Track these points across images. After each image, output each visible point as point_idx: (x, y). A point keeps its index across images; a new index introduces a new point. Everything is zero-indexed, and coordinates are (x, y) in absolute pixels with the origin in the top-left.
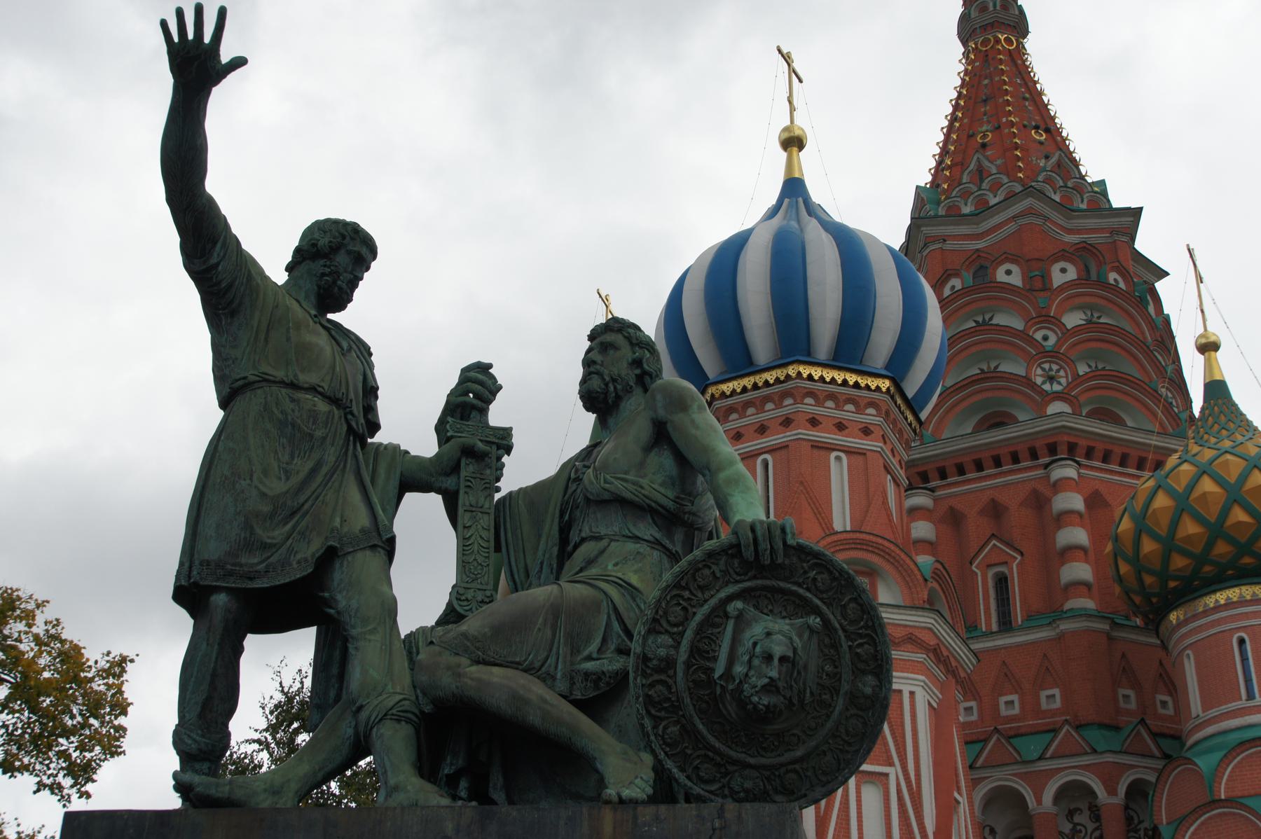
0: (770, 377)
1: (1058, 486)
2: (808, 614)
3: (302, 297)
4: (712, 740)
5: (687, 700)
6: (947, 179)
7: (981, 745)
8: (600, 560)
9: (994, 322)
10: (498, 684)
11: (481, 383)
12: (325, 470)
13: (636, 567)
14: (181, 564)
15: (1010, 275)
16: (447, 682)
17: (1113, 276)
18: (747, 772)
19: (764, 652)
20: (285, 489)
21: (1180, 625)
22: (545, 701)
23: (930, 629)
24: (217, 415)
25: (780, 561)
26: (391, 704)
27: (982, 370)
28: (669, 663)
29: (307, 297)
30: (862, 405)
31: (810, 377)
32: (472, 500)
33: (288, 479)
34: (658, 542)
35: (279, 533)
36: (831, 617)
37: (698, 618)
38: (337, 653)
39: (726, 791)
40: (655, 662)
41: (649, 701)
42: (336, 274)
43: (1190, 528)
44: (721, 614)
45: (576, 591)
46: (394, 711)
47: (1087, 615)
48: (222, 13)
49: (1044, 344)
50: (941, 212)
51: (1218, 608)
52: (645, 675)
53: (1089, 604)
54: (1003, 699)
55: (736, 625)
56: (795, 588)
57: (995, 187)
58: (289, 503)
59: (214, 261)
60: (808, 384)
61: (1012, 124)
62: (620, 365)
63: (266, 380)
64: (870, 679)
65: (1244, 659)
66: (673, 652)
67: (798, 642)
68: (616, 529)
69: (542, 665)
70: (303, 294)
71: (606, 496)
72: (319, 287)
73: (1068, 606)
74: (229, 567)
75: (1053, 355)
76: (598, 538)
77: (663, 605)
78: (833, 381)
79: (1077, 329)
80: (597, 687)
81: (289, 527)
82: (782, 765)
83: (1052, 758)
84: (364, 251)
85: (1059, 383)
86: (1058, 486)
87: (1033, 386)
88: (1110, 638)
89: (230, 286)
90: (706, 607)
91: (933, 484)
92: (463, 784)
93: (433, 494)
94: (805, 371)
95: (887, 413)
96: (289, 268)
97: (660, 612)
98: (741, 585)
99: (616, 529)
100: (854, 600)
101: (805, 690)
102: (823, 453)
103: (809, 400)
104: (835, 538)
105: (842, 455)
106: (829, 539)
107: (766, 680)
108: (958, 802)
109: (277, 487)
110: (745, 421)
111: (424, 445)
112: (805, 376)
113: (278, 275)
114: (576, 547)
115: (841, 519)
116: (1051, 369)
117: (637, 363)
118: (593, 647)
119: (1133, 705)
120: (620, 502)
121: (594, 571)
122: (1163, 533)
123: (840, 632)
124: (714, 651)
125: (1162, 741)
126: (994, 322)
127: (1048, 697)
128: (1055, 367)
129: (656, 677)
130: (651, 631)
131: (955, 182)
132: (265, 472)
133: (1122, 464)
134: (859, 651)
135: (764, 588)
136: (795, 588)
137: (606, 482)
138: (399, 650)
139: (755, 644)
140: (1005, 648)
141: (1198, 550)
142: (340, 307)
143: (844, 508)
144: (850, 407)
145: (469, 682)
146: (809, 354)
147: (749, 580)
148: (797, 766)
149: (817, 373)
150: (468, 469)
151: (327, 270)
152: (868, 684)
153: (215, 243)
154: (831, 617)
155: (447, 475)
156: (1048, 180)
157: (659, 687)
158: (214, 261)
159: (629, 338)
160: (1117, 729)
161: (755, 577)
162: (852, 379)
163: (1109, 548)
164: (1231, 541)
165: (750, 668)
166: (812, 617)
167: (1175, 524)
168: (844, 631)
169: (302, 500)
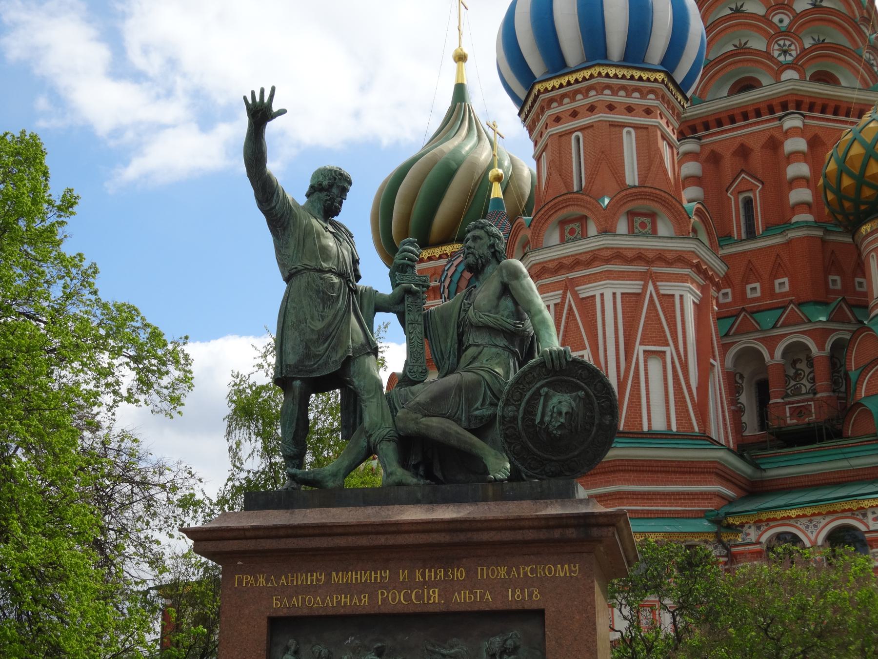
0: (579, 76)
1: (788, 134)
2: (578, 390)
3: (316, 213)
4: (535, 450)
5: (524, 434)
7: (734, 319)
8: (479, 357)
9: (743, 9)
10: (435, 425)
16: (412, 427)
21: (869, 235)
22: (458, 433)
23: (693, 252)
27: (735, 46)
28: (515, 418)
29: (319, 212)
30: (645, 92)
31: (607, 75)
35: (322, 348)
37: (527, 397)
41: (506, 436)
42: (332, 200)
45: (469, 376)
47: (806, 225)
48: (273, 89)
49: (779, 25)
53: (809, 218)
54: (749, 287)
59: (273, 205)
60: (607, 80)
63: (307, 269)
64: (608, 417)
67: (574, 404)
71: (480, 324)
73: (794, 220)
75: (786, 33)
76: (478, 346)
78: (624, 77)
79: (805, 12)
81: (326, 345)
83: (781, 326)
85: (791, 55)
86: (788, 134)
87: (771, 58)
88: (823, 241)
89: (282, 215)
91: (700, 134)
93: (391, 313)
95: (663, 97)
96: (308, 196)
100: (600, 381)
102: (617, 129)
103: (607, 92)
104: (627, 192)
105: (631, 130)
108: (713, 366)
109: (319, 325)
110: (562, 108)
112: (604, 74)
113: (302, 200)
114: (467, 348)
115: (631, 177)
116: (784, 45)
117: (492, 246)
118: (478, 404)
119: (839, 286)
121: (476, 364)
122: (856, 172)
126: (743, 9)
127: (780, 284)
128: (788, 43)
132: (312, 318)
133: (835, 113)
138: (385, 403)
140: (751, 251)
142: (337, 215)
143: (633, 168)
144: (636, 95)
146: (606, 57)
149: (612, 72)
150: (409, 300)
152: (607, 420)
155: (398, 304)
158: (273, 205)
162: (637, 74)
163: (821, 182)
167: (865, 166)
168: (595, 396)
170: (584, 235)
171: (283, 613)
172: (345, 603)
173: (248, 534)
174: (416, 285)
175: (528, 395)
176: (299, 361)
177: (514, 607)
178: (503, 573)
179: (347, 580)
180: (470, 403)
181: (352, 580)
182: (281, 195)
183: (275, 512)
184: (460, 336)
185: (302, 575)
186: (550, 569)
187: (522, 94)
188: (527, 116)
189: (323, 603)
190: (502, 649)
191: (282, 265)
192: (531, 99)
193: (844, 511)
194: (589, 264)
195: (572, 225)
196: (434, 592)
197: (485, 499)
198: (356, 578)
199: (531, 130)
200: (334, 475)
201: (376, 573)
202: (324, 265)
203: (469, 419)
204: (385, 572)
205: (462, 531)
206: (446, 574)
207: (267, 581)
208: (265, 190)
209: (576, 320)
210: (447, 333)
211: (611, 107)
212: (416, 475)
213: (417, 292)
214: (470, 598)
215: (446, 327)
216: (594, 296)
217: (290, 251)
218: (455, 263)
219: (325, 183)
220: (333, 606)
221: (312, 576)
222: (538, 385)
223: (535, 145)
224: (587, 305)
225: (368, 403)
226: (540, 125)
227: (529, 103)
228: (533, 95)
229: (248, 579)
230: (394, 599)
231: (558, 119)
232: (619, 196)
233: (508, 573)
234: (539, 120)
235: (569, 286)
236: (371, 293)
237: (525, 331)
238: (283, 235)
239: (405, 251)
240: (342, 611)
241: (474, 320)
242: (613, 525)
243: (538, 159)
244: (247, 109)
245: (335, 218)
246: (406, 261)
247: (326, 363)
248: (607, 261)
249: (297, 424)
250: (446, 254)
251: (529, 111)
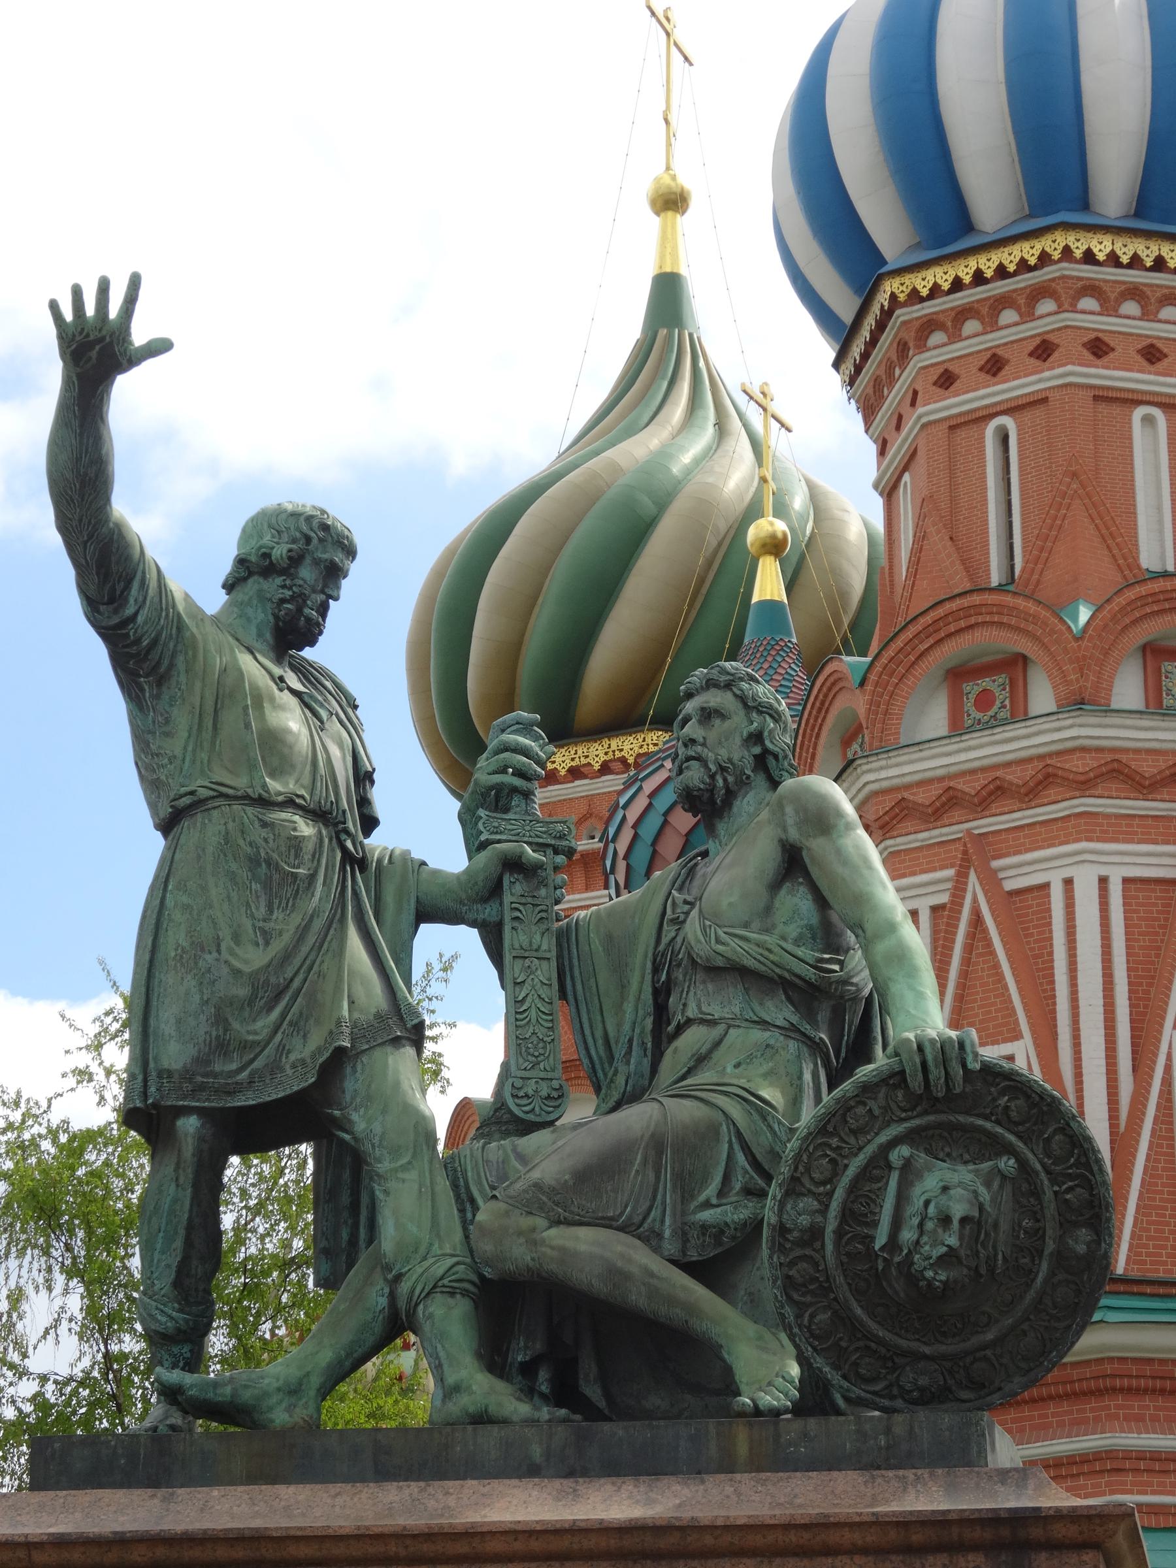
0: (1009, 257)
2: (999, 1155)
3: (250, 640)
4: (873, 1325)
5: (840, 1280)
8: (716, 1055)
10: (588, 1250)
13: (766, 1067)
16: (519, 1255)
18: (922, 1364)
19: (940, 1211)
20: (266, 960)
22: (652, 1275)
24: (152, 845)
25: (958, 1091)
26: (440, 1272)
28: (815, 1234)
29: (260, 635)
31: (1089, 257)
32: (523, 938)
33: (267, 943)
34: (793, 1028)
36: (1030, 1156)
37: (851, 1172)
38: (347, 1175)
39: (895, 1391)
40: (796, 1234)
41: (789, 1284)
42: (300, 599)
44: (882, 1163)
45: (685, 1111)
46: (445, 1282)
48: (135, 283)
52: (782, 1249)
55: (900, 1176)
56: (980, 1122)
58: (273, 980)
59: (130, 611)
60: (1087, 272)
64: (1084, 1234)
66: (819, 1219)
67: (985, 1195)
68: (737, 1010)
69: (645, 1219)
70: (254, 630)
71: (720, 962)
72: (276, 617)
74: (199, 1079)
76: (712, 1023)
77: (805, 1157)
80: (719, 1243)
84: (338, 557)
89: (155, 642)
90: (861, 1156)
92: (543, 1375)
94: (1079, 243)
96: (230, 586)
97: (801, 1168)
98: (907, 1125)
99: (737, 1010)
100: (1061, 1130)
101: (996, 1255)
102: (1116, 410)
104: (1142, 590)
105: (1157, 412)
106: (1131, 594)
107: (945, 1249)
109: (254, 958)
112: (1078, 254)
114: (680, 1029)
117: (757, 737)
118: (710, 1192)
121: (705, 1076)
123: (1043, 1175)
124: (875, 1214)
129: (798, 1252)
132: (236, 938)
134: (1068, 1197)
135: (939, 1125)
136: (980, 1122)
137: (718, 941)
138: (443, 1184)
139: (927, 1203)
142: (312, 642)
143: (1161, 522)
145: (549, 1251)
146: (1085, 205)
147: (917, 1116)
148: (988, 1352)
149: (1102, 246)
150: (514, 889)
151: (288, 593)
154: (1030, 1156)
158: (130, 611)
159: (742, 699)
161: (926, 1113)
165: (922, 1233)
166: (1005, 1158)
168: (1048, 1172)
169: (289, 974)
170: (1019, 713)
174: (539, 847)
176: (197, 1060)
180: (686, 1187)
182: (153, 584)
183: (120, 1496)
187: (844, 305)
188: (858, 369)
191: (152, 783)
192: (870, 322)
194: (1030, 794)
195: (985, 683)
197: (727, 1466)
199: (868, 410)
200: (293, 1390)
202: (274, 785)
203: (683, 1234)
208: (107, 570)
209: (993, 953)
210: (623, 987)
211: (1098, 348)
212: (529, 1393)
213: (539, 866)
215: (620, 968)
216: (1046, 886)
217: (175, 746)
218: (649, 786)
219: (280, 552)
222: (883, 1138)
223: (882, 452)
224: (1025, 910)
225: (392, 1185)
226: (895, 396)
227: (865, 333)
228: (875, 310)
231: (946, 380)
232: (1121, 600)
234: (892, 380)
235: (974, 856)
237: (846, 982)
238: (157, 697)
239: (506, 748)
241: (702, 948)
242: (1096, 1546)
243: (889, 491)
244: (61, 337)
245: (308, 653)
246: (509, 779)
247: (274, 1067)
248: (1084, 785)
249: (188, 1243)
250: (623, 760)
251: (865, 356)
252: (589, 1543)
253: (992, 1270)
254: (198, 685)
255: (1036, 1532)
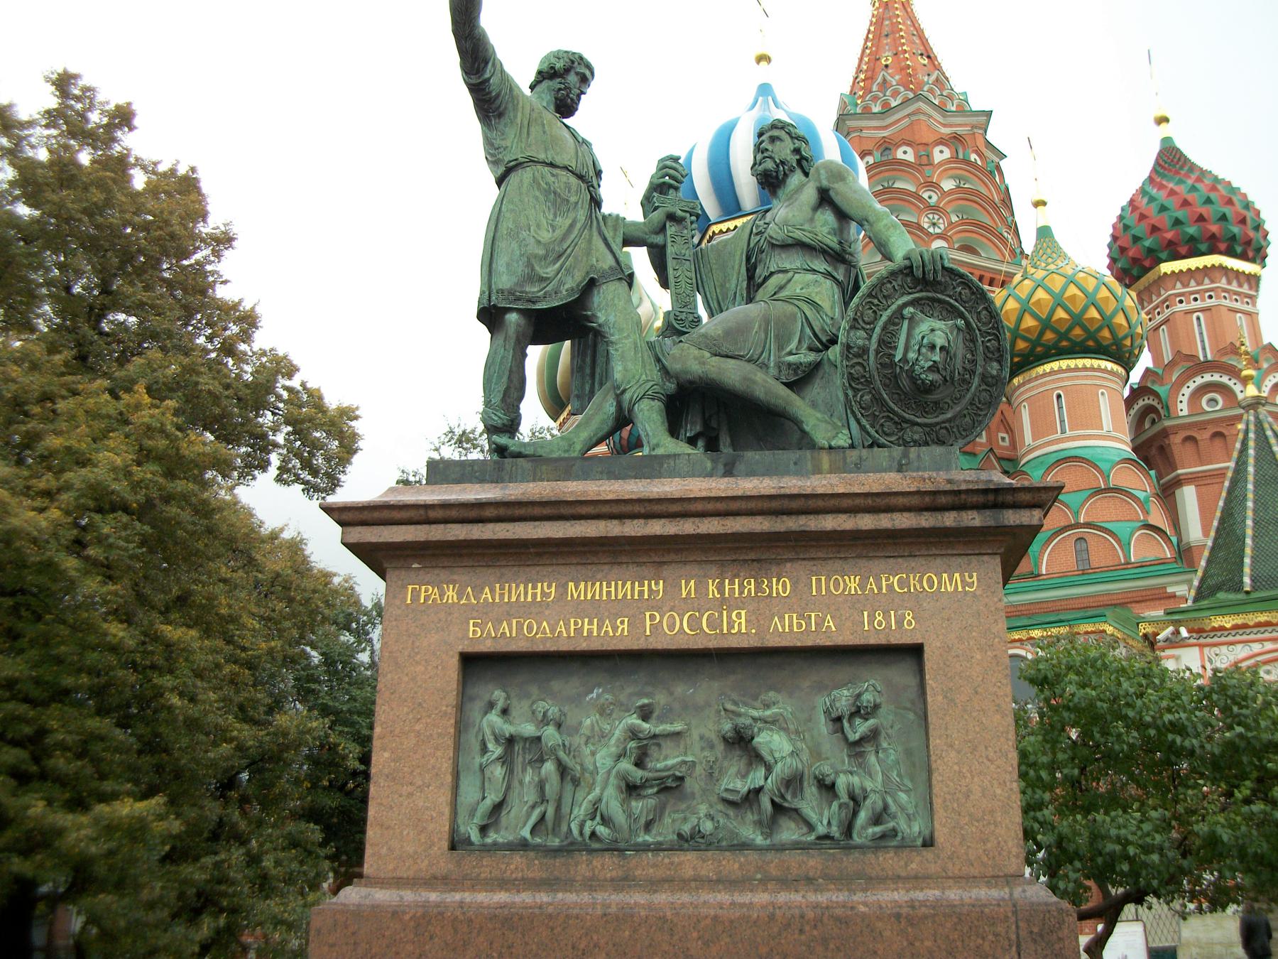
2: (956, 318)
6: (862, 88)
11: (675, 169)
12: (579, 225)
14: (482, 293)
15: (906, 154)
17: (973, 157)
18: (915, 428)
21: (1020, 386)
24: (492, 192)
28: (865, 350)
35: (550, 271)
37: (884, 318)
38: (588, 360)
41: (851, 377)
43: (1029, 322)
50: (859, 110)
51: (1045, 375)
52: (848, 358)
57: (895, 94)
59: (487, 75)
61: (905, 52)
62: (784, 150)
63: (532, 161)
64: (995, 364)
65: (1060, 408)
71: (790, 241)
75: (935, 209)
76: (786, 271)
79: (951, 192)
80: (796, 373)
81: (558, 265)
82: (937, 424)
84: (588, 73)
87: (921, 229)
89: (498, 95)
96: (532, 87)
100: (986, 309)
109: (546, 236)
111: (634, 214)
114: (766, 279)
117: (797, 151)
118: (793, 346)
120: (800, 245)
125: (1003, 463)
129: (855, 360)
130: (853, 327)
131: (868, 90)
132: (538, 226)
141: (1034, 337)
150: (671, 229)
153: (487, 63)
155: (657, 233)
156: (931, 91)
157: (858, 368)
158: (487, 75)
159: (789, 134)
160: (975, 455)
161: (921, 291)
164: (1055, 331)
171: (487, 647)
172: (590, 632)
173: (432, 514)
175: (885, 316)
177: (872, 641)
178: (853, 585)
179: (594, 595)
180: (782, 342)
181: (601, 595)
182: (498, 67)
184: (751, 271)
185: (517, 587)
186: (930, 579)
189: (553, 631)
190: (853, 709)
191: (493, 161)
193: (1015, 641)
196: (739, 616)
197: (817, 470)
198: (609, 593)
201: (642, 585)
203: (779, 366)
204: (657, 584)
205: (790, 513)
206: (758, 588)
207: (460, 595)
214: (800, 626)
220: (569, 637)
221: (534, 588)
222: (900, 302)
229: (428, 592)
230: (671, 627)
233: (862, 586)
236: (618, 220)
240: (584, 646)
252: (752, 505)
253: (952, 378)
254: (519, 115)
255: (1009, 498)
